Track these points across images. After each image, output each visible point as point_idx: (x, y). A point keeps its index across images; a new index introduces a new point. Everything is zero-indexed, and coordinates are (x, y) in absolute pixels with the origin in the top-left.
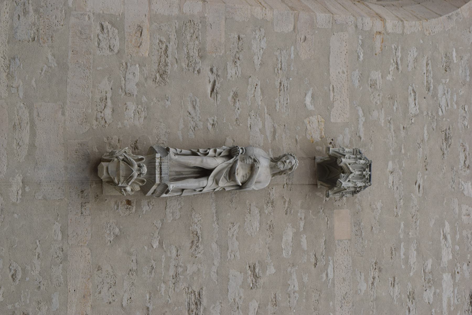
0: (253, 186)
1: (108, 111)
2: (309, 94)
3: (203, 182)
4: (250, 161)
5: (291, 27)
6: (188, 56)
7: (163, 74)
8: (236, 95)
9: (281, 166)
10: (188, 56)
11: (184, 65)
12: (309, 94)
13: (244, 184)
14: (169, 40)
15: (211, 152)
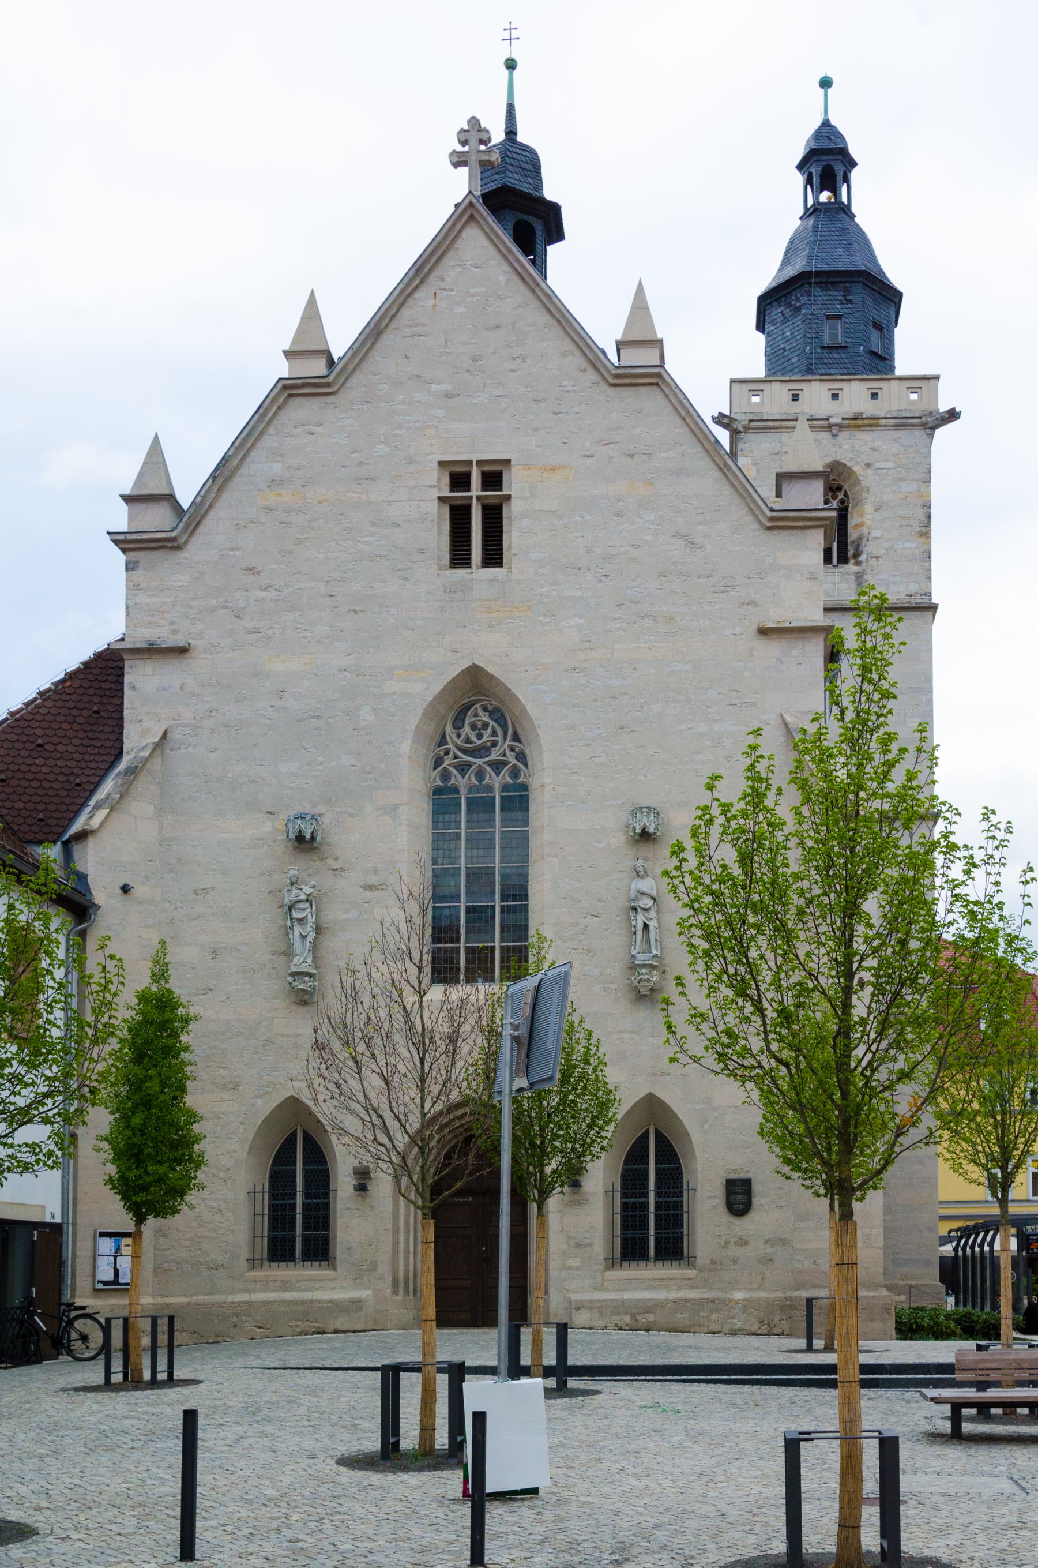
0: (654, 893)
1: (612, 986)
2: (596, 845)
3: (651, 928)
4: (639, 896)
5: (555, 860)
6: (577, 934)
7: (589, 951)
8: (599, 900)
9: (642, 873)
10: (577, 934)
11: (583, 937)
12: (596, 845)
13: (653, 898)
14: (568, 948)
15: (634, 923)
